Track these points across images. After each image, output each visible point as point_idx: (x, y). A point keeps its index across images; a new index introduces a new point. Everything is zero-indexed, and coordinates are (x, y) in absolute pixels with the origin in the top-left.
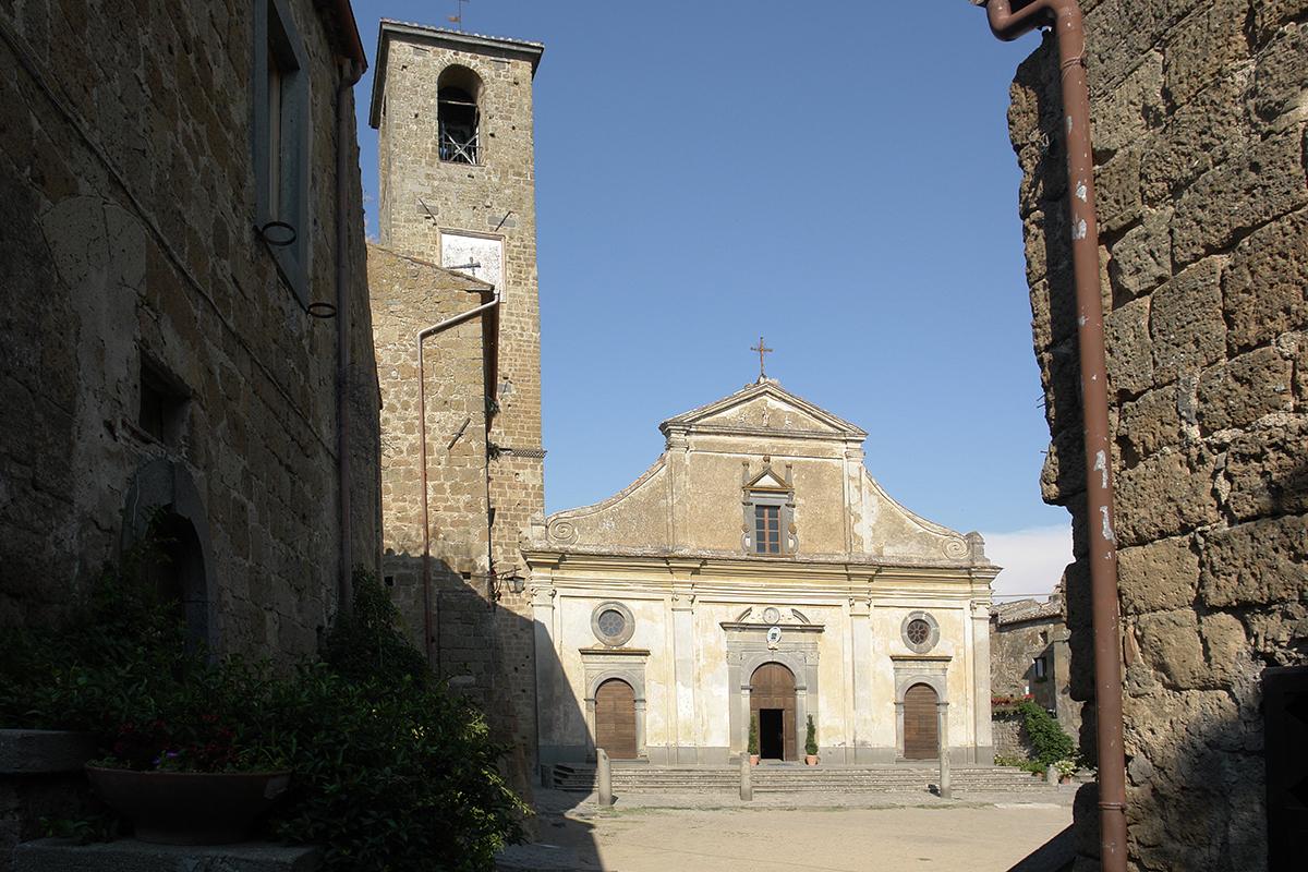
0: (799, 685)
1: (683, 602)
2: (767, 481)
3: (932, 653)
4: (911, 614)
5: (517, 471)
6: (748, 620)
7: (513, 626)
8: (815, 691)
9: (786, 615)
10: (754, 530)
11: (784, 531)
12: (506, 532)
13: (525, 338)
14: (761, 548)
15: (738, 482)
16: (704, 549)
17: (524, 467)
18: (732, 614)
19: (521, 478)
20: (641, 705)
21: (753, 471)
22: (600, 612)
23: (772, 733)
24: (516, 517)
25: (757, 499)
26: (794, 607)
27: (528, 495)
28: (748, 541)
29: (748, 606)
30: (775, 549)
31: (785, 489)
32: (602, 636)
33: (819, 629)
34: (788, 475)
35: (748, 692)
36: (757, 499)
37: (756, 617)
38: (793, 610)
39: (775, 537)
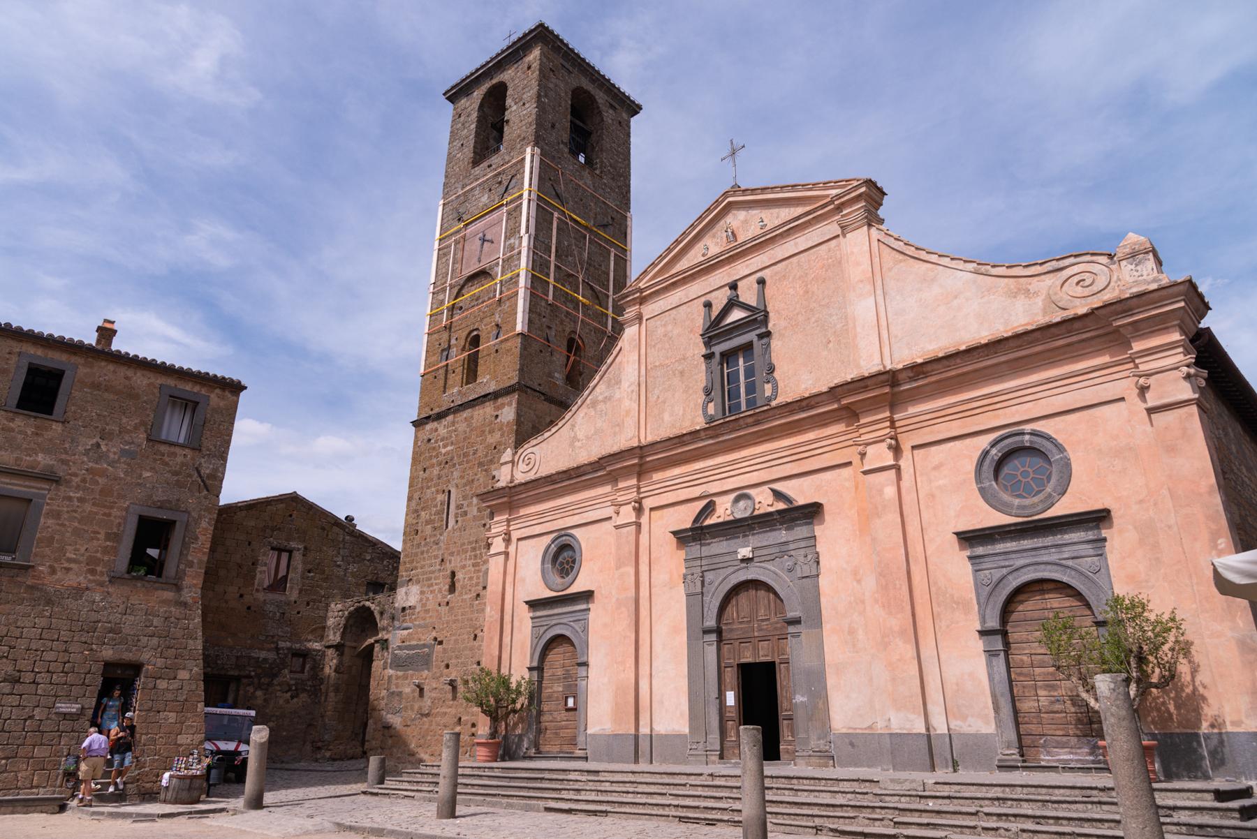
0: (791, 614)
1: (628, 514)
2: (737, 315)
3: (1061, 508)
4: (994, 444)
6: (710, 521)
7: (477, 584)
8: (817, 621)
9: (764, 502)
11: (760, 374)
17: (503, 405)
18: (684, 518)
20: (582, 671)
22: (553, 548)
23: (759, 701)
24: (491, 462)
25: (718, 349)
26: (778, 486)
27: (502, 435)
28: (711, 409)
31: (758, 318)
33: (813, 512)
34: (762, 296)
35: (713, 637)
36: (718, 349)
37: (724, 511)
38: (772, 490)
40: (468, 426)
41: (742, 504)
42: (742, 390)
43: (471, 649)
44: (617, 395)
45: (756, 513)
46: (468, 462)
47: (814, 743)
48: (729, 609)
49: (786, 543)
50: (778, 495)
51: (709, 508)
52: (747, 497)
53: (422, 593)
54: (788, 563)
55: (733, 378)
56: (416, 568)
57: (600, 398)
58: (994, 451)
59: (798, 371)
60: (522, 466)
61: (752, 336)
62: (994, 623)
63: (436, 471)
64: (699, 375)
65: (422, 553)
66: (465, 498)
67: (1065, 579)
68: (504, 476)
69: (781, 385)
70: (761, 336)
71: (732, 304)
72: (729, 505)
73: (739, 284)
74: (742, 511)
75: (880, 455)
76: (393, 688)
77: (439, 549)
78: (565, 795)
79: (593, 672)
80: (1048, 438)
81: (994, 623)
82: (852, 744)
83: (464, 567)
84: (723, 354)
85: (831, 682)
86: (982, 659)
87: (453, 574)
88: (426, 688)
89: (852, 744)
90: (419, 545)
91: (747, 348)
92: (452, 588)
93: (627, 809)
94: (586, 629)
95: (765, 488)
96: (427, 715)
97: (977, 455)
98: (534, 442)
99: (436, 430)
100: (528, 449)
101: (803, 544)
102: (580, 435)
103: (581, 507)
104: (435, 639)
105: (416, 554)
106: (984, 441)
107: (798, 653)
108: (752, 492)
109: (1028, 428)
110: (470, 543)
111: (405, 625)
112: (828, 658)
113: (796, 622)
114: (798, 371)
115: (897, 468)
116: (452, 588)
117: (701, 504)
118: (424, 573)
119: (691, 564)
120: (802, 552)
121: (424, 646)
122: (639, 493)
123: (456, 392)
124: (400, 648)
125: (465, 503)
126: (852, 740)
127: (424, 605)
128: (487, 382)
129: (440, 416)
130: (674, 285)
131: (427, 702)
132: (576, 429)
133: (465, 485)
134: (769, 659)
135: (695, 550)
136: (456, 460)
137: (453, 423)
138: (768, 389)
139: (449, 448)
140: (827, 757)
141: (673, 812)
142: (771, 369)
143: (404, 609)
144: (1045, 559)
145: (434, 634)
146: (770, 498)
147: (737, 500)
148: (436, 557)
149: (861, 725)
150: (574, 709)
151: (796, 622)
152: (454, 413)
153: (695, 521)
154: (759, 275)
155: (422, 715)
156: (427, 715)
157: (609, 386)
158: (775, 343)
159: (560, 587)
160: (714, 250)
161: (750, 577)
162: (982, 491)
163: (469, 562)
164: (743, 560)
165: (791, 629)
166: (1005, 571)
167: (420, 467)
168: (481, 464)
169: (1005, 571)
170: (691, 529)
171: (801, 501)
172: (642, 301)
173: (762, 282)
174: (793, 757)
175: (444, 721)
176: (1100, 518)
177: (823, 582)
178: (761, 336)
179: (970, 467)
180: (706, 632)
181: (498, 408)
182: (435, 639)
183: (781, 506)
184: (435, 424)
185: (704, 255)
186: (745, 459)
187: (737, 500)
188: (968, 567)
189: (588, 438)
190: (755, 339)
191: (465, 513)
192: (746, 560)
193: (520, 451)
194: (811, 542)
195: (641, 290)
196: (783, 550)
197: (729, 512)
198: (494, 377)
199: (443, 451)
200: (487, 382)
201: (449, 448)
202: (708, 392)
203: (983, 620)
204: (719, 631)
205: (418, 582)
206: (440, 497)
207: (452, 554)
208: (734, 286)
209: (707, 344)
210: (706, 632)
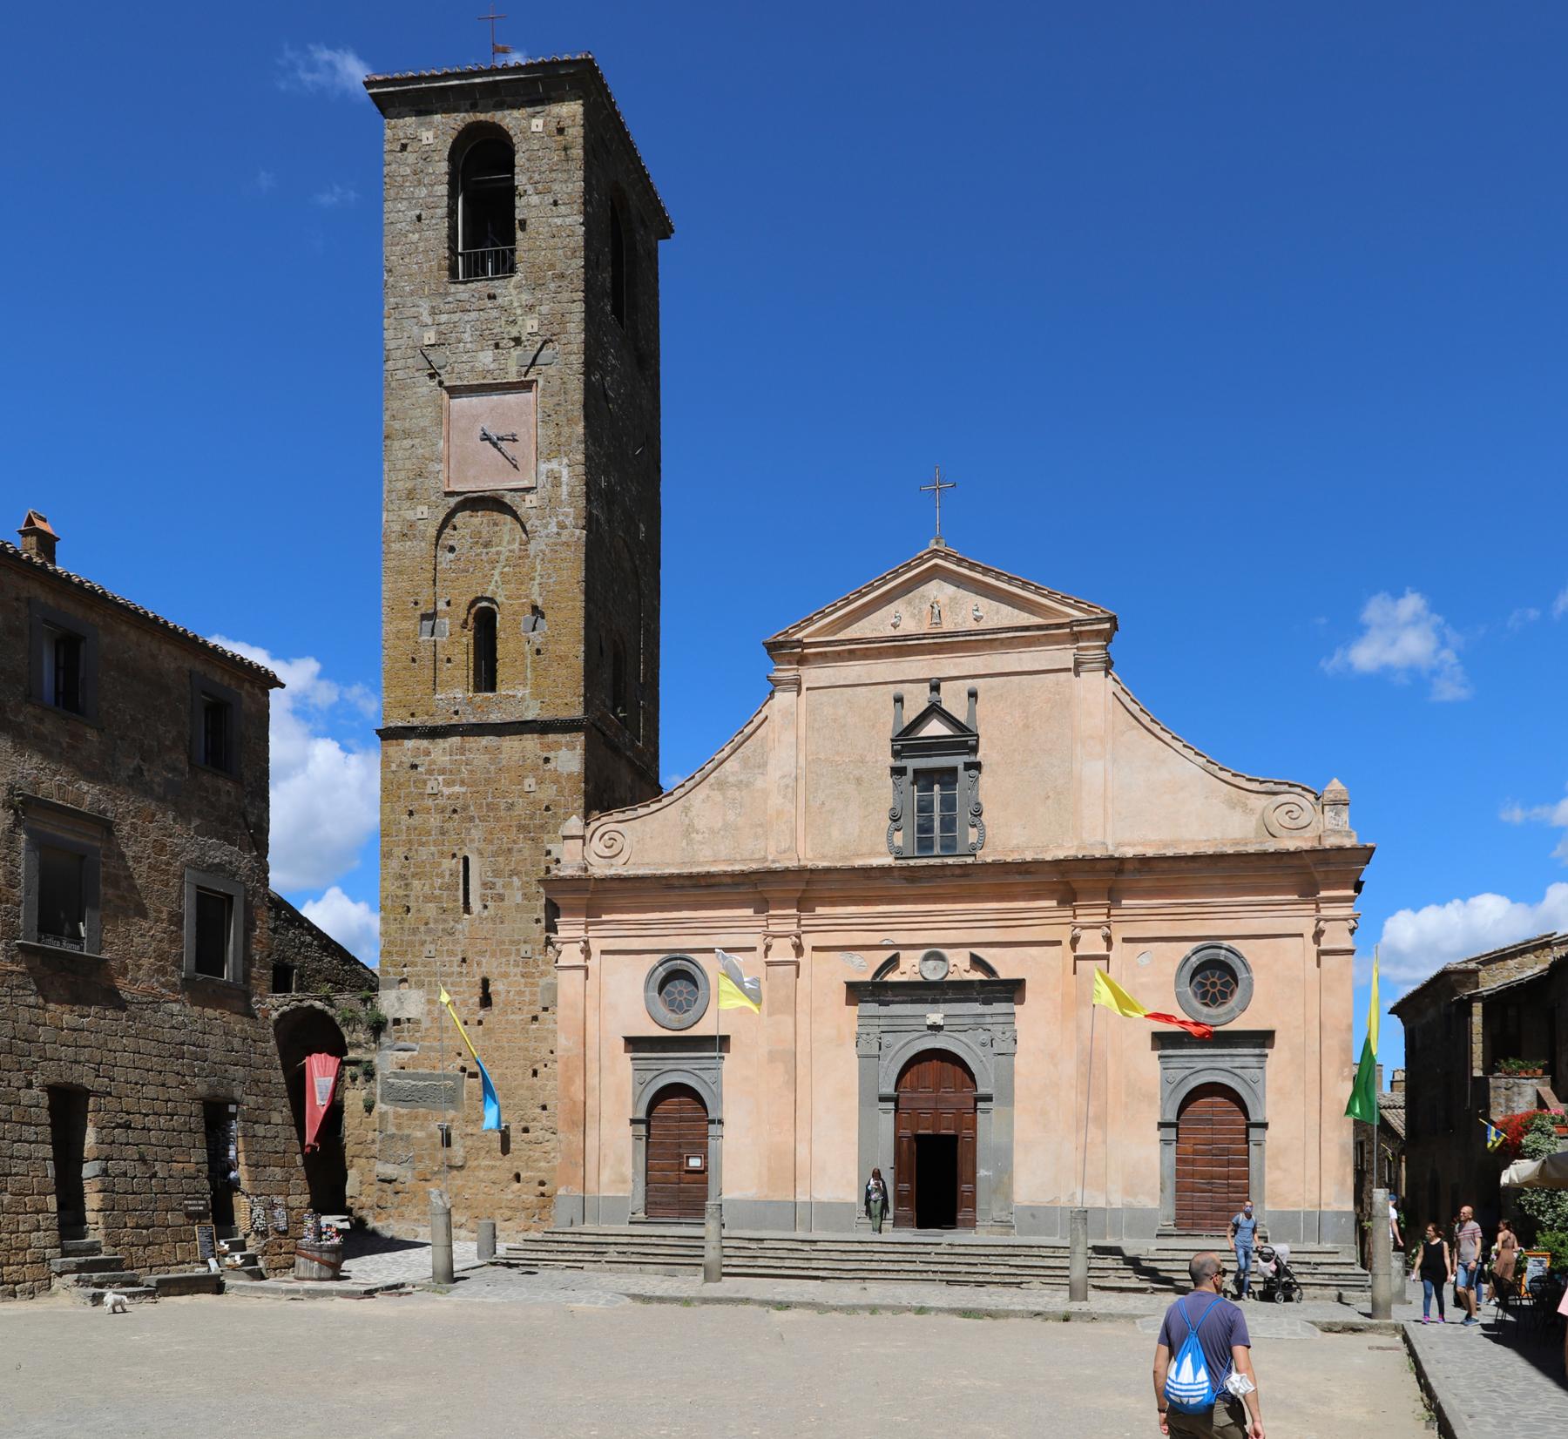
0: (982, 1090)
2: (936, 728)
5: (545, 755)
6: (892, 977)
8: (1009, 1100)
9: (959, 967)
10: (911, 820)
11: (962, 814)
12: (526, 853)
13: (564, 539)
14: (925, 845)
15: (887, 732)
16: (824, 857)
17: (556, 746)
18: (863, 968)
19: (550, 766)
21: (910, 714)
24: (542, 827)
25: (912, 764)
26: (978, 951)
27: (560, 792)
28: (898, 839)
29: (891, 953)
30: (949, 846)
31: (964, 740)
32: (662, 1011)
33: (1013, 990)
34: (972, 713)
35: (891, 1105)
37: (910, 968)
39: (948, 825)
40: (492, 761)
41: (931, 963)
42: (937, 824)
43: (530, 1088)
44: (759, 783)
45: (950, 978)
46: (498, 820)
47: (997, 1214)
48: (908, 1075)
49: (983, 1015)
50: (977, 962)
51: (892, 963)
52: (941, 958)
53: (429, 1001)
54: (985, 1037)
55: (925, 808)
56: (414, 964)
57: (732, 779)
58: (1194, 959)
59: (1012, 820)
60: (597, 845)
61: (958, 761)
62: (1171, 1117)
63: (434, 821)
64: (885, 791)
65: (423, 943)
66: (497, 873)
67: (1232, 1085)
68: (570, 860)
69: (989, 832)
70: (969, 766)
71: (934, 710)
72: (917, 961)
73: (943, 685)
74: (933, 972)
75: (1092, 942)
76: (392, 1130)
77: (456, 942)
78: (814, 1264)
79: (727, 1130)
80: (1239, 957)
81: (1171, 1117)
82: (1033, 1216)
83: (505, 975)
84: (916, 771)
85: (1018, 1157)
86: (1158, 1145)
87: (485, 983)
88: (454, 1134)
89: (1033, 1216)
90: (415, 931)
91: (948, 777)
92: (486, 1001)
93: (879, 1275)
94: (718, 1082)
95: (966, 952)
96: (461, 1167)
97: (1180, 959)
98: (618, 816)
99: (428, 753)
100: (608, 823)
101: (1001, 1019)
102: (700, 824)
103: (710, 928)
104: (463, 1070)
105: (411, 944)
106: (1189, 947)
107: (988, 1129)
108: (945, 951)
109: (1226, 943)
110: (512, 942)
111: (402, 1044)
112: (1017, 1135)
113: (989, 1098)
114: (1010, 826)
115: (1106, 958)
116: (486, 1001)
117: (886, 955)
118: (429, 974)
119: (866, 1021)
120: (1000, 1027)
121: (446, 1077)
122: (799, 925)
123: (455, 696)
124: (396, 1075)
125: (499, 882)
126: (1033, 1212)
127: (434, 1020)
128: (519, 695)
129: (434, 733)
130: (852, 655)
131: (458, 1151)
132: (693, 813)
133: (495, 854)
134: (952, 1132)
135: (872, 1008)
136: (472, 811)
137: (462, 750)
138: (973, 835)
139: (457, 789)
140: (1007, 1226)
141: (939, 1276)
142: (978, 813)
143: (397, 1022)
144: (1221, 1065)
145: (460, 1062)
146: (967, 965)
147: (927, 958)
148: (451, 953)
149: (1043, 1199)
150: (702, 1172)
151: (989, 1098)
152: (462, 735)
153: (877, 974)
154: (970, 683)
155: (451, 1167)
156: (461, 1167)
157: (745, 763)
158: (985, 779)
159: (676, 1025)
160: (909, 626)
161: (938, 1046)
162: (1178, 994)
163: (513, 970)
164: (930, 1027)
165: (980, 1105)
166: (1187, 1072)
167: (401, 806)
168: (522, 828)
169: (1187, 1072)
170: (872, 983)
171: (1003, 974)
172: (802, 660)
173: (973, 695)
174: (971, 1224)
175: (493, 1175)
176: (1264, 1039)
177: (1017, 1060)
178: (969, 766)
179: (1172, 969)
180: (883, 1099)
181: (549, 748)
182: (463, 1070)
183: (978, 976)
184: (424, 743)
185: (895, 626)
186: (942, 913)
187: (927, 958)
188: (1157, 1065)
189: (712, 831)
190: (961, 767)
191: (501, 898)
192: (935, 1028)
193: (594, 825)
194: (1009, 1019)
195: (800, 643)
196: (978, 1023)
197: (916, 969)
198: (536, 695)
199: (446, 791)
200: (519, 695)
201: (457, 789)
202: (895, 819)
203: (1163, 1115)
204: (896, 1100)
205: (420, 985)
206: (449, 864)
207: (482, 953)
208: (935, 688)
209: (896, 754)
210: (883, 1099)
